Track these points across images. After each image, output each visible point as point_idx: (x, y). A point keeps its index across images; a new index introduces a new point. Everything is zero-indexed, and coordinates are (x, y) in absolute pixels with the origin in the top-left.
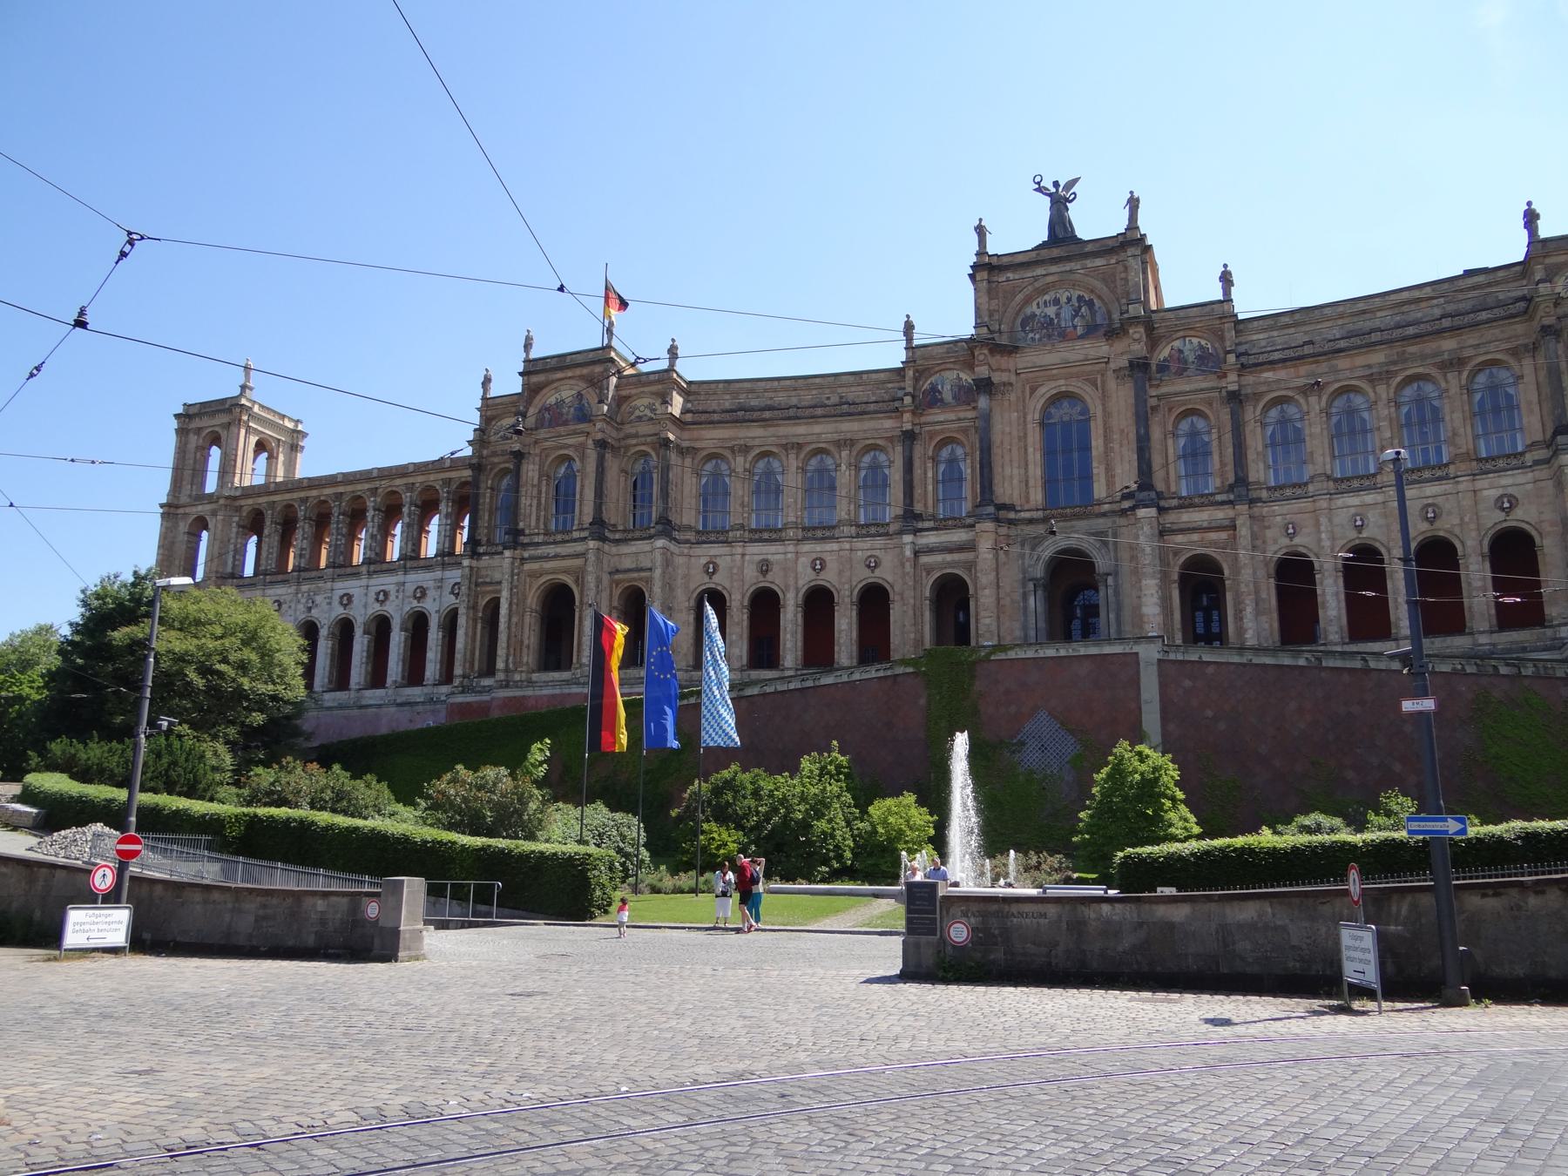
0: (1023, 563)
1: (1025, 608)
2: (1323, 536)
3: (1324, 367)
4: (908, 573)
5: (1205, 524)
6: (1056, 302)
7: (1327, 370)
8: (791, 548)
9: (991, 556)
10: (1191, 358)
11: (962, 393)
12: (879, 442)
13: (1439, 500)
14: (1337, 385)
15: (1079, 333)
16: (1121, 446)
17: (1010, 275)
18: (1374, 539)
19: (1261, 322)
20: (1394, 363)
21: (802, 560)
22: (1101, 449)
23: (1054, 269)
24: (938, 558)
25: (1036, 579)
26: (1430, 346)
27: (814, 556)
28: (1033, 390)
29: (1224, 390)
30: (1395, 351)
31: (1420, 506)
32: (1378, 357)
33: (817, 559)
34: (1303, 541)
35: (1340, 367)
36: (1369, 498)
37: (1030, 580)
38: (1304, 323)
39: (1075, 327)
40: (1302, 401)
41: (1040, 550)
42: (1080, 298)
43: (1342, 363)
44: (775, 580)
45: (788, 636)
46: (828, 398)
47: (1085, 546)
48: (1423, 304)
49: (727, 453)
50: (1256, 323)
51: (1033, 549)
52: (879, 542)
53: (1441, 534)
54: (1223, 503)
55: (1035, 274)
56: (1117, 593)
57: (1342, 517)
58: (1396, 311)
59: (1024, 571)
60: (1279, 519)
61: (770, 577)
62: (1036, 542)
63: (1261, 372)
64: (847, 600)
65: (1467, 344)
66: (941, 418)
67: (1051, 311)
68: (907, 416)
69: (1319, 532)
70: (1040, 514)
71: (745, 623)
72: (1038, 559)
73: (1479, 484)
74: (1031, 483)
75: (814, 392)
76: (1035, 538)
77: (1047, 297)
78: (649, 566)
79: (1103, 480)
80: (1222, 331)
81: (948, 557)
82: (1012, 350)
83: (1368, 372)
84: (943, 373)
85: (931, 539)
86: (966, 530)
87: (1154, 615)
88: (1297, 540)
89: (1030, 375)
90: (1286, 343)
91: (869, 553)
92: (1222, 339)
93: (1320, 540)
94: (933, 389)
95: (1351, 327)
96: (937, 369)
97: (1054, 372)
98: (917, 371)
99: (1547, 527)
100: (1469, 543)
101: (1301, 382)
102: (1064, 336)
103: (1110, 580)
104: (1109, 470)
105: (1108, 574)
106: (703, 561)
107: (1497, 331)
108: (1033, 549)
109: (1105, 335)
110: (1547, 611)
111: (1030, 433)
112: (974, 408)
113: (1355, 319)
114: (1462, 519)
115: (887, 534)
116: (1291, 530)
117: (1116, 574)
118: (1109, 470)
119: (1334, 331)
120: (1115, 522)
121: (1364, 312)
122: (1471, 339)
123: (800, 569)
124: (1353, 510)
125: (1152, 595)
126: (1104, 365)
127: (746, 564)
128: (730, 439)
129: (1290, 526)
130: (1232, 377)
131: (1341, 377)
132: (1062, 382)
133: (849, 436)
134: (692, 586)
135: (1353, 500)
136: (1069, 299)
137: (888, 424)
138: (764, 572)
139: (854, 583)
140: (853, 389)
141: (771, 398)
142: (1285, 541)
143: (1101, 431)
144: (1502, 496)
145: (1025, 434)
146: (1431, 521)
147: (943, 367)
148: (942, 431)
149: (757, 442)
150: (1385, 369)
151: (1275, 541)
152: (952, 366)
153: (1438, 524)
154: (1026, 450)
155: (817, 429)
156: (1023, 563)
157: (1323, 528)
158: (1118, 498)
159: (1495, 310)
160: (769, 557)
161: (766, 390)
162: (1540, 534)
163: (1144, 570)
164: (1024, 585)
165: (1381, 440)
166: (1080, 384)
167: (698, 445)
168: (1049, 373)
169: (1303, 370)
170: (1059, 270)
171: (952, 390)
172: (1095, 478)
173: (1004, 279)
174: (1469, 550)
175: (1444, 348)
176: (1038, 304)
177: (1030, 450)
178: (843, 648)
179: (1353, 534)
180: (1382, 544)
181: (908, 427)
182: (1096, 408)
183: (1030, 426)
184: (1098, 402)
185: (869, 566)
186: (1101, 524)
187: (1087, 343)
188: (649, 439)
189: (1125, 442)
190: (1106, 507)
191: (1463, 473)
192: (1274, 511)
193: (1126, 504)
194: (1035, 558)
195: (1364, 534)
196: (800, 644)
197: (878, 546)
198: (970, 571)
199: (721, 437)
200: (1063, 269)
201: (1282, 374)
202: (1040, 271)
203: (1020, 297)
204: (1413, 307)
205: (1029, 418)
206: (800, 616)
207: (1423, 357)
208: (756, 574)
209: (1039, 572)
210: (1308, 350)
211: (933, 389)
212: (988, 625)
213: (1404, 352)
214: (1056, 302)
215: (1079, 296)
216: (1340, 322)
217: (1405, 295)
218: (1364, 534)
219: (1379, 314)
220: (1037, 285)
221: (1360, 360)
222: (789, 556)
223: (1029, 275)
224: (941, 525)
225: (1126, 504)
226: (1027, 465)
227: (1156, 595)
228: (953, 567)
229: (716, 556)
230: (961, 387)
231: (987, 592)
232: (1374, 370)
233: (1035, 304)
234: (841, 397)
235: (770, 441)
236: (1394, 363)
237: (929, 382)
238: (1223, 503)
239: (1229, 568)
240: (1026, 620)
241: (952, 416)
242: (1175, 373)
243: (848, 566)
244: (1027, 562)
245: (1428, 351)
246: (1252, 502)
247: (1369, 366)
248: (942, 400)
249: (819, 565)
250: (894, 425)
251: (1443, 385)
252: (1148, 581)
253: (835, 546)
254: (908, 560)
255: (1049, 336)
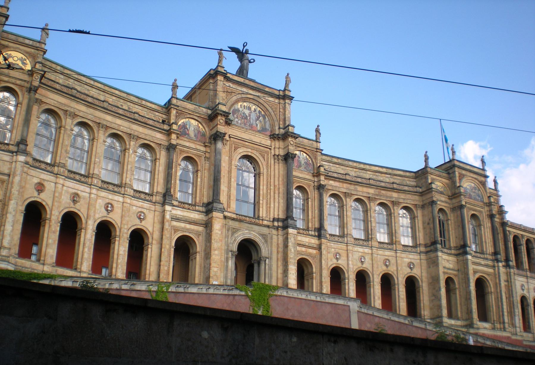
0: (227, 241)
1: (227, 266)
2: (350, 262)
3: (352, 187)
4: (167, 229)
5: (307, 244)
6: (249, 108)
7: (353, 189)
8: (94, 191)
9: (220, 232)
10: (303, 162)
11: (199, 134)
12: (152, 144)
13: (390, 258)
14: (356, 197)
15: (258, 129)
16: (274, 193)
17: (231, 85)
18: (367, 269)
19: (326, 157)
20: (377, 195)
21: (99, 201)
22: (265, 191)
23: (251, 92)
24: (182, 225)
25: (234, 252)
26: (389, 193)
27: (107, 201)
28: (236, 149)
29: (315, 183)
30: (377, 190)
31: (384, 259)
32: (371, 191)
33: (109, 203)
34: (342, 263)
35: (358, 189)
36: (367, 250)
37: (231, 251)
38: (342, 165)
39: (257, 125)
40: (343, 199)
41: (236, 235)
42: (260, 112)
43: (359, 188)
44: (81, 209)
45: (86, 250)
46: (122, 105)
47: (257, 240)
48: (383, 175)
49: (61, 113)
50: (324, 156)
51: (232, 235)
52: (146, 205)
53: (390, 273)
54: (312, 235)
55: (242, 90)
56: (270, 269)
57: (357, 256)
58: (374, 173)
59: (228, 246)
60: (333, 250)
61: (78, 205)
62: (235, 231)
63: (331, 180)
64: (125, 235)
65: (401, 197)
66: (187, 144)
67: (247, 112)
68: (174, 136)
69: (348, 260)
70: (234, 216)
71: (58, 233)
72: (235, 240)
73: (403, 255)
74: (232, 198)
75: (114, 98)
76: (234, 228)
77: (245, 104)
78: (6, 171)
79: (264, 208)
80: (316, 155)
81: (188, 226)
82: (228, 123)
83: (368, 196)
84: (190, 120)
85: (179, 212)
86: (199, 213)
87: (294, 284)
88: (339, 262)
89: (235, 140)
90: (335, 170)
91: (140, 210)
92: (316, 158)
93: (348, 264)
94: (184, 126)
95: (359, 174)
96: (189, 116)
97: (247, 143)
98: (177, 113)
99: (424, 279)
100: (400, 279)
101: (345, 191)
102: (252, 128)
103: (267, 260)
104: (268, 204)
105: (267, 258)
106: (36, 181)
107: (410, 196)
108: (232, 235)
109: (270, 136)
110: (422, 312)
111: (233, 171)
112: (205, 146)
113: (360, 171)
114: (397, 268)
115: (151, 201)
116: (337, 256)
117: (270, 258)
118: (268, 204)
119: (353, 173)
120: (271, 231)
121: (363, 169)
122: (402, 196)
123: (97, 207)
124: (360, 254)
125: (293, 274)
126: (268, 150)
127: (63, 192)
128: (65, 105)
129: (338, 254)
130: (322, 178)
131: (358, 193)
132: (250, 150)
133: (136, 134)
134: (26, 196)
135: (361, 250)
136: (255, 110)
137: (159, 136)
138: (75, 202)
139: (130, 226)
140: (137, 106)
141: (88, 90)
142: (335, 261)
143: (265, 182)
144: (411, 262)
145: (231, 170)
146: (387, 266)
147: (192, 116)
148: (187, 152)
149: (81, 114)
150: (374, 196)
151: (331, 260)
152: (196, 118)
153: (389, 268)
154: (231, 179)
155: (119, 121)
156: (227, 241)
157: (350, 259)
158: (271, 220)
159: (410, 187)
160: (79, 192)
161: (87, 84)
162: (422, 281)
163: (291, 260)
164: (227, 254)
165: (371, 226)
166: (257, 155)
167: (44, 100)
168: (244, 143)
169: (345, 185)
170: (253, 94)
171: (194, 131)
172: (261, 206)
173: (228, 85)
174: (400, 282)
175: (394, 196)
176: (241, 105)
177: (232, 180)
178: (119, 266)
179: (360, 264)
180: (370, 272)
181: (174, 142)
182: (263, 169)
183: (233, 167)
184: (265, 167)
185: (140, 218)
186: (265, 230)
187: (261, 136)
188: (18, 82)
189: (277, 192)
190: (265, 223)
191: (399, 249)
192: (331, 245)
193: (276, 224)
194: (233, 239)
195: (364, 266)
196: (91, 257)
197: (146, 207)
198: (198, 237)
199: (60, 101)
200: (255, 94)
201: (336, 184)
202: (245, 90)
203: (234, 98)
204: (380, 174)
205: (233, 162)
206: (94, 237)
207: (387, 197)
208: (69, 201)
209: (235, 248)
210: (348, 177)
211: (184, 126)
212: (216, 272)
213: (380, 192)
214: (249, 108)
215: (259, 111)
216: (355, 170)
217: (377, 169)
218: (364, 266)
219: (368, 172)
220: (243, 96)
221: (365, 189)
222: (93, 196)
223: (240, 89)
224: (182, 205)
225: (276, 224)
226: (230, 187)
227: (294, 274)
228: (190, 233)
229: (44, 180)
230: (199, 132)
231: (216, 252)
232: (370, 196)
233: (240, 104)
234: (129, 108)
235: (90, 117)
236: (377, 195)
237: (182, 121)
238: (312, 235)
239: (316, 268)
240: (227, 274)
241: (192, 145)
242: (296, 166)
243: (127, 214)
244: (229, 240)
245: (388, 195)
246: (326, 238)
247: (369, 193)
248: (188, 134)
249: (109, 207)
250: (162, 138)
251: (392, 211)
252: (292, 267)
253: (121, 199)
254: (168, 221)
255: (245, 124)
